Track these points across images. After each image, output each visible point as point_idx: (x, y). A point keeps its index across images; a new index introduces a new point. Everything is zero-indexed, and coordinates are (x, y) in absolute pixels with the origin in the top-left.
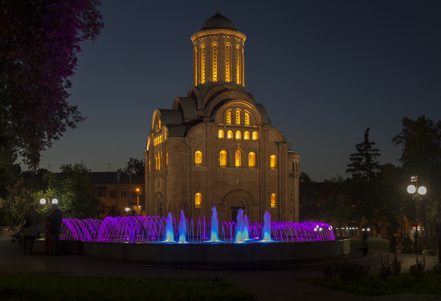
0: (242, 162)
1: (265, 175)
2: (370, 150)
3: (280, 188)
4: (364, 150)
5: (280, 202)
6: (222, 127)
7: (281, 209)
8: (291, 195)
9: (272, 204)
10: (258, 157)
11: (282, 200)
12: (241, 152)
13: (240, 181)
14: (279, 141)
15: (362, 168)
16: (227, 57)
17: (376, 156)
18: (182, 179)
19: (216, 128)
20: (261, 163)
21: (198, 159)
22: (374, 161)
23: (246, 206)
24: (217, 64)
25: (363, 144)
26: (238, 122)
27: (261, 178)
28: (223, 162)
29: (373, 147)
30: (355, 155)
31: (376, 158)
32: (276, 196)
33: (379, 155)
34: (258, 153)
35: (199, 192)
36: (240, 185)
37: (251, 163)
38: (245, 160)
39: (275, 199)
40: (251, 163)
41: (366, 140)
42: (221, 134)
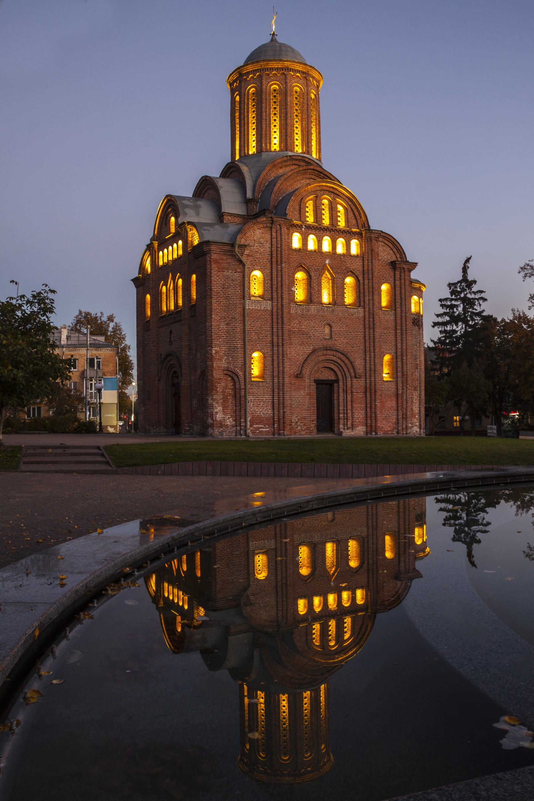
0: (333, 295)
1: (374, 321)
2: (470, 293)
3: (399, 345)
4: (460, 293)
5: (399, 370)
6: (298, 228)
7: (400, 385)
8: (415, 359)
9: (384, 375)
10: (362, 287)
11: (402, 366)
12: (332, 276)
13: (331, 331)
14: (394, 259)
15: (455, 320)
16: (296, 110)
17: (481, 302)
18: (227, 324)
19: (288, 229)
20: (367, 298)
21: (256, 286)
22: (476, 310)
23: (340, 377)
24: (280, 120)
25: (458, 282)
26: (326, 221)
27: (367, 326)
28: (300, 294)
29: (475, 288)
30: (446, 299)
31: (480, 305)
32: (392, 359)
33: (485, 300)
34: (361, 278)
35: (258, 350)
36: (331, 338)
37: (349, 298)
38: (338, 291)
39: (389, 365)
40: (349, 298)
41: (465, 279)
42: (296, 241)
